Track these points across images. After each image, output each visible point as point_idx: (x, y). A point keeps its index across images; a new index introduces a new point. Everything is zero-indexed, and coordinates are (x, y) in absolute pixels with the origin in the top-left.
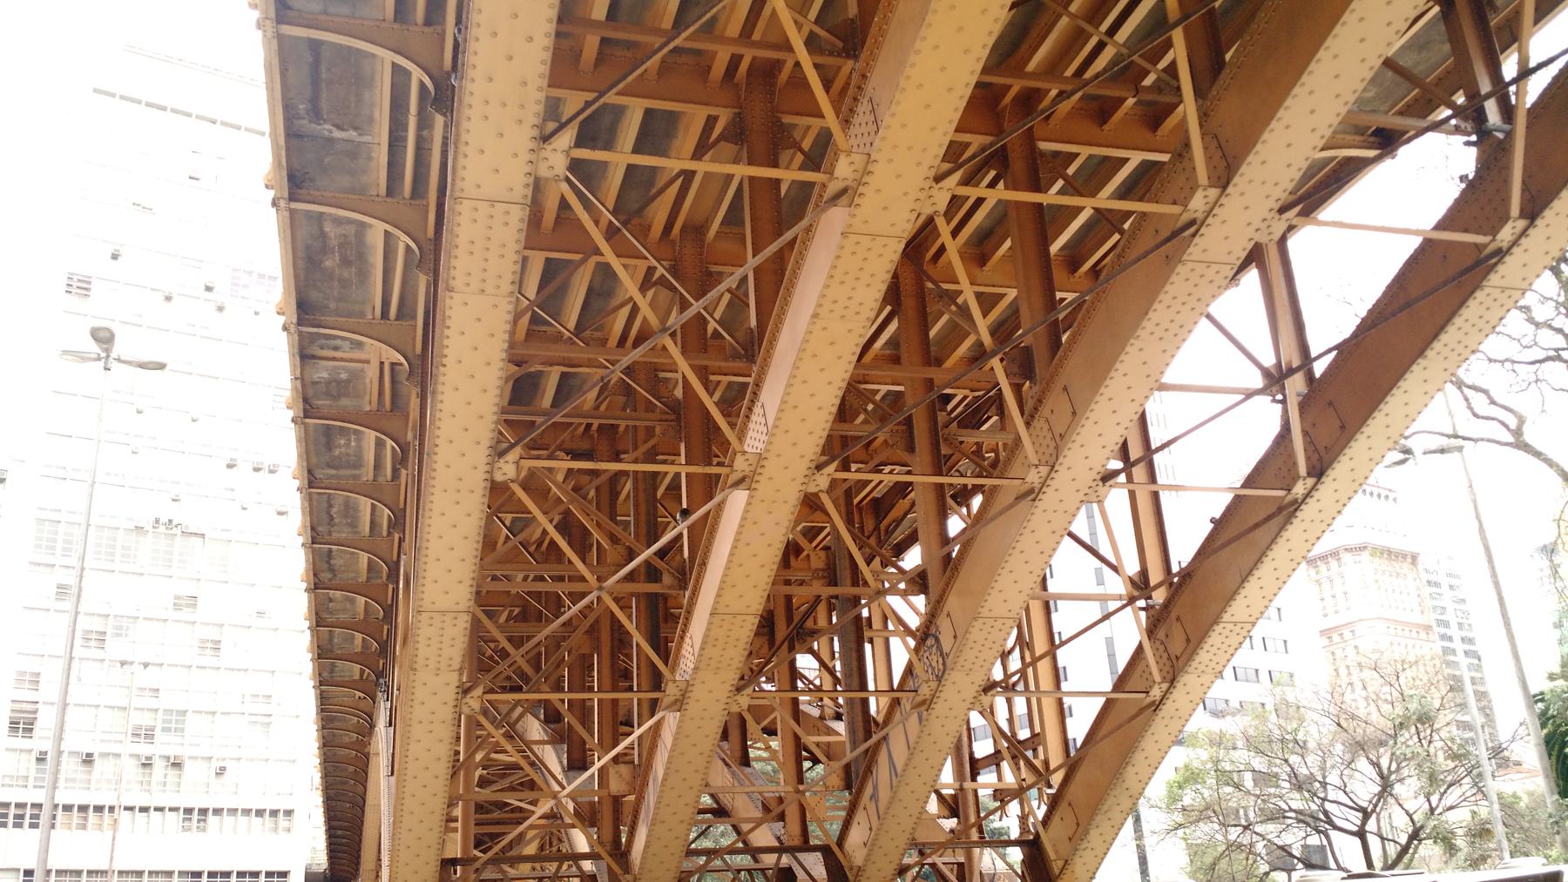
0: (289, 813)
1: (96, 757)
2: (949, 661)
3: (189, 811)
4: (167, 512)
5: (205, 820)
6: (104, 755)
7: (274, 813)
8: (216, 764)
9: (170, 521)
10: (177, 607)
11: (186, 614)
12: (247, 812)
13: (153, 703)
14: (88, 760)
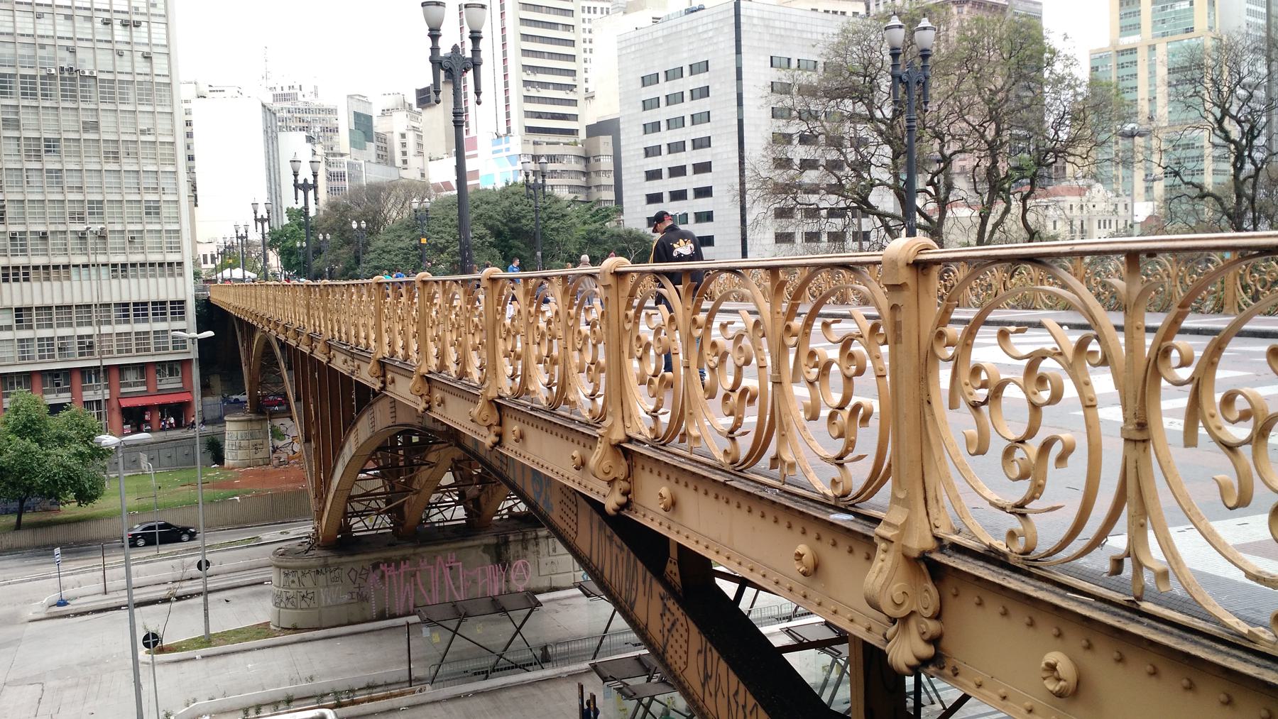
0: (180, 264)
1: (48, 233)
3: (114, 265)
4: (66, 60)
6: (52, 232)
7: (170, 264)
8: (128, 235)
9: (71, 68)
10: (86, 130)
11: (91, 136)
12: (152, 265)
13: (79, 197)
14: (44, 236)
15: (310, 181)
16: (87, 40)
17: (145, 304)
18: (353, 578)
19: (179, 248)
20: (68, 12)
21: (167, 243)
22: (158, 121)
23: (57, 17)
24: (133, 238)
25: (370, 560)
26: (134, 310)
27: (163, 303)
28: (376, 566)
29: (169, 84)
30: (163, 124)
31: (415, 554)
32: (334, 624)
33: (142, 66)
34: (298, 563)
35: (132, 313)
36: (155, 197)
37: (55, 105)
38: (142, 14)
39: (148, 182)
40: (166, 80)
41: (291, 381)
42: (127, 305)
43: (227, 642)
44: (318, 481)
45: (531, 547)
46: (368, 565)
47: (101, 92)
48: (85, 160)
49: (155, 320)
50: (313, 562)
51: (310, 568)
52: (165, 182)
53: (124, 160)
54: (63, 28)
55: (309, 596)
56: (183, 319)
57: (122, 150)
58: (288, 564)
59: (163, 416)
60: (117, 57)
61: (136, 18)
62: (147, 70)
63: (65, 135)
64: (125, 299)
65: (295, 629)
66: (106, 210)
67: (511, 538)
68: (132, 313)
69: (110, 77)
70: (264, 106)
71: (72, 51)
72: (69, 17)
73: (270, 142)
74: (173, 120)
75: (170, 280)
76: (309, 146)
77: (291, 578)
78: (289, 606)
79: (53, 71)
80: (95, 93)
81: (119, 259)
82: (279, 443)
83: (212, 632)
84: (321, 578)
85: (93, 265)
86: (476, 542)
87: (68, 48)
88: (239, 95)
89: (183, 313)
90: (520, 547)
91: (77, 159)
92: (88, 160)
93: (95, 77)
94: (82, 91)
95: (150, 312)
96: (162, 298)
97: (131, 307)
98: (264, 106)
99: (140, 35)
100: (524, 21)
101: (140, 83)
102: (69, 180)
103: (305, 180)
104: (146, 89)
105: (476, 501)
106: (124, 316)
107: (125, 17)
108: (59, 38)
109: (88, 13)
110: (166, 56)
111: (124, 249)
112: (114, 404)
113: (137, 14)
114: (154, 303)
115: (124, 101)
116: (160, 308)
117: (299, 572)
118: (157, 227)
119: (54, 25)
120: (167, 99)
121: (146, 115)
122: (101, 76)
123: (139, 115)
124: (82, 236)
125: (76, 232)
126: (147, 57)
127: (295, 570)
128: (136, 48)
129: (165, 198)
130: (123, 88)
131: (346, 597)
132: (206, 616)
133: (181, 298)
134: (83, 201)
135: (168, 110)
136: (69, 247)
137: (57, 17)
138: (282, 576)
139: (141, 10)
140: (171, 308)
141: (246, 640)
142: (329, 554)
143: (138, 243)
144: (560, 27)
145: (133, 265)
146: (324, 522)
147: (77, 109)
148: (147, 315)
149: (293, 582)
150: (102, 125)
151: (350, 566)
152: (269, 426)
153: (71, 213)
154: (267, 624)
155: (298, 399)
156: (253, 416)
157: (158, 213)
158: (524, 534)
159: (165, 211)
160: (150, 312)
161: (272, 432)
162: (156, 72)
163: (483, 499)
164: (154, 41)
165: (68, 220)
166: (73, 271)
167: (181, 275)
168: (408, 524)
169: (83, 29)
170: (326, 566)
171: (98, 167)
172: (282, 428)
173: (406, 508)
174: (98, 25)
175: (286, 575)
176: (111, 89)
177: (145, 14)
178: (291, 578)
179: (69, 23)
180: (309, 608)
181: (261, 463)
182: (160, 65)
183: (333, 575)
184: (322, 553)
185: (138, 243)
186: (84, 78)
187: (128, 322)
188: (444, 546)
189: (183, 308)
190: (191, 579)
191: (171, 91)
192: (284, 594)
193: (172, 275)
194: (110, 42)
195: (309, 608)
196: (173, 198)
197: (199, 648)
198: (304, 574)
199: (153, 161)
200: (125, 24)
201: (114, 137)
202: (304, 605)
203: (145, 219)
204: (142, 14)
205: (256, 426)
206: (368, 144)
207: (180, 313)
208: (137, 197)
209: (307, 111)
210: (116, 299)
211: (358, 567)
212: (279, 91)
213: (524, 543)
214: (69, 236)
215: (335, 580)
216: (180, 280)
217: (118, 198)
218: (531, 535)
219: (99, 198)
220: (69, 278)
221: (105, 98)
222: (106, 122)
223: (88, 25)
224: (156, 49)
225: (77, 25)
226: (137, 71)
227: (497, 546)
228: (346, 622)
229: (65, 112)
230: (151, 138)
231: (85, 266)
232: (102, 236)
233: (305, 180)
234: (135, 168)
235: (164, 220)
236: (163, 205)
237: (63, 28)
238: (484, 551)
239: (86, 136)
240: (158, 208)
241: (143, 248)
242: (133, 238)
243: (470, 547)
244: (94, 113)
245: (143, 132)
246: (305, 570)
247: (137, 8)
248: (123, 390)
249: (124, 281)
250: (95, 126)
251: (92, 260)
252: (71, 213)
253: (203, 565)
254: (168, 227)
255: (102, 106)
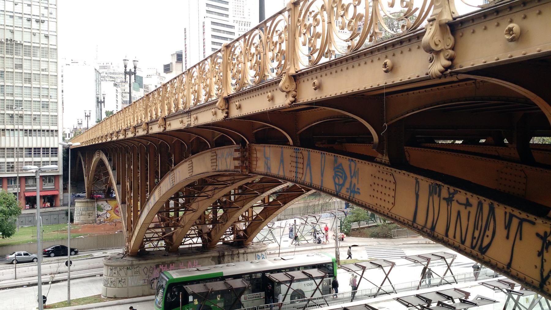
0: (57, 131)
2: (229, 219)
3: (26, 130)
4: (9, 36)
5: (31, 133)
7: (52, 131)
8: (33, 117)
9: (11, 40)
10: (16, 68)
12: (44, 131)
13: (12, 98)
15: (133, 70)
16: (19, 27)
17: (39, 149)
18: (146, 272)
19: (57, 123)
20: (12, 14)
21: (51, 121)
22: (50, 66)
23: (6, 16)
24: (35, 118)
25: (154, 263)
26: (34, 151)
27: (48, 148)
28: (157, 266)
29: (56, 49)
30: (52, 67)
31: (177, 261)
32: (136, 296)
33: (44, 40)
34: (118, 263)
35: (33, 152)
36: (47, 100)
37: (3, 56)
38: (45, 17)
39: (45, 93)
40: (55, 47)
41: (114, 175)
42: (31, 149)
43: (79, 304)
44: (130, 222)
45: (236, 258)
46: (154, 266)
47: (25, 51)
48: (15, 81)
49: (43, 156)
50: (126, 263)
51: (124, 266)
52: (52, 93)
53: (33, 82)
54: (9, 21)
55: (123, 281)
56: (56, 156)
57: (33, 77)
58: (112, 264)
59: (44, 201)
60: (33, 36)
61: (42, 19)
62: (47, 43)
63: (6, 70)
64: (30, 146)
65: (115, 298)
66: (24, 105)
67: (226, 253)
68: (33, 152)
69: (29, 44)
70: (96, 70)
71: (12, 32)
72: (12, 17)
73: (98, 85)
74: (57, 65)
75: (52, 138)
76: (115, 88)
77: (114, 271)
78: (112, 286)
79: (3, 40)
80: (22, 52)
81: (28, 127)
82: (100, 213)
83: (71, 299)
84: (129, 272)
85: (17, 130)
86: (209, 255)
87: (10, 30)
88: (85, 64)
89: (57, 153)
90: (230, 258)
91: (12, 81)
92: (17, 81)
93: (22, 44)
94: (16, 50)
95: (41, 152)
96: (47, 146)
97: (33, 150)
98: (96, 70)
99: (44, 26)
100: (213, 36)
101: (43, 48)
102: (7, 90)
103: (130, 70)
104: (46, 51)
105: (209, 234)
106: (29, 154)
107: (38, 18)
108: (7, 26)
109: (20, 15)
110: (55, 37)
111: (31, 123)
112: (22, 195)
113: (43, 17)
114: (43, 148)
115: (35, 55)
116: (46, 151)
117: (118, 268)
118: (47, 114)
119: (4, 20)
120: (55, 56)
121: (45, 63)
122: (25, 44)
123: (41, 62)
124: (12, 116)
125: (9, 114)
126: (47, 37)
127: (116, 267)
128: (42, 32)
129: (51, 100)
130: (35, 50)
131: (142, 282)
132: (69, 290)
133: (56, 146)
134: (13, 100)
135: (55, 61)
136: (5, 121)
137: (6, 16)
138: (109, 270)
139: (45, 16)
140: (51, 151)
141: (89, 303)
142: (134, 259)
143: (38, 120)
144: (229, 39)
145: (35, 130)
146: (132, 242)
147: (13, 58)
148: (40, 154)
149: (115, 273)
150: (24, 66)
151: (146, 266)
152: (96, 205)
153: (7, 105)
154: (100, 295)
155: (118, 183)
156: (89, 200)
157: (48, 107)
158: (232, 252)
159: (51, 106)
160: (41, 152)
161: (97, 208)
162: (50, 43)
163: (213, 233)
164: (50, 30)
165: (6, 109)
166: (6, 132)
167: (57, 136)
168: (175, 245)
169: (18, 22)
170: (132, 265)
171: (21, 85)
172: (102, 206)
173: (174, 237)
174: (25, 20)
175: (111, 270)
176: (29, 50)
177: (47, 17)
178: (114, 271)
179: (11, 19)
180: (122, 287)
181: (91, 222)
182: (52, 40)
183: (135, 270)
184: (130, 259)
185: (38, 120)
186: (17, 44)
187: (31, 157)
188: (193, 257)
189: (57, 151)
190: (59, 273)
191: (57, 52)
192: (110, 279)
193: (53, 136)
194: (30, 29)
195: (122, 287)
196: (56, 101)
197: (65, 306)
198: (120, 270)
199: (47, 83)
200: (37, 21)
201: (29, 72)
202: (120, 285)
203: (42, 110)
204: (45, 17)
205: (90, 205)
206: (140, 89)
207: (55, 153)
208: (39, 100)
209: (114, 73)
210: (26, 146)
211: (148, 267)
212: (102, 65)
213: (232, 256)
214: (6, 116)
215: (136, 273)
216: (56, 138)
217: (30, 99)
218: (236, 252)
219: (21, 99)
220: (4, 135)
221: (26, 54)
222: (26, 65)
223: (20, 21)
224: (50, 33)
225: (15, 20)
226: (42, 42)
227: (219, 257)
228: (141, 295)
229: (7, 59)
230: (47, 73)
231: (12, 130)
232: (21, 117)
233: (130, 70)
234: (38, 86)
235: (50, 111)
236: (50, 104)
237: (9, 21)
238: (212, 260)
239: (16, 70)
240: (48, 105)
241: (40, 123)
242: (35, 118)
243: (206, 257)
244: (21, 60)
245: (43, 70)
246: (121, 267)
247: (43, 15)
248: (27, 188)
249: (30, 138)
250: (21, 66)
251: (16, 127)
252: (7, 105)
253: (69, 263)
254: (52, 114)
255: (24, 57)
